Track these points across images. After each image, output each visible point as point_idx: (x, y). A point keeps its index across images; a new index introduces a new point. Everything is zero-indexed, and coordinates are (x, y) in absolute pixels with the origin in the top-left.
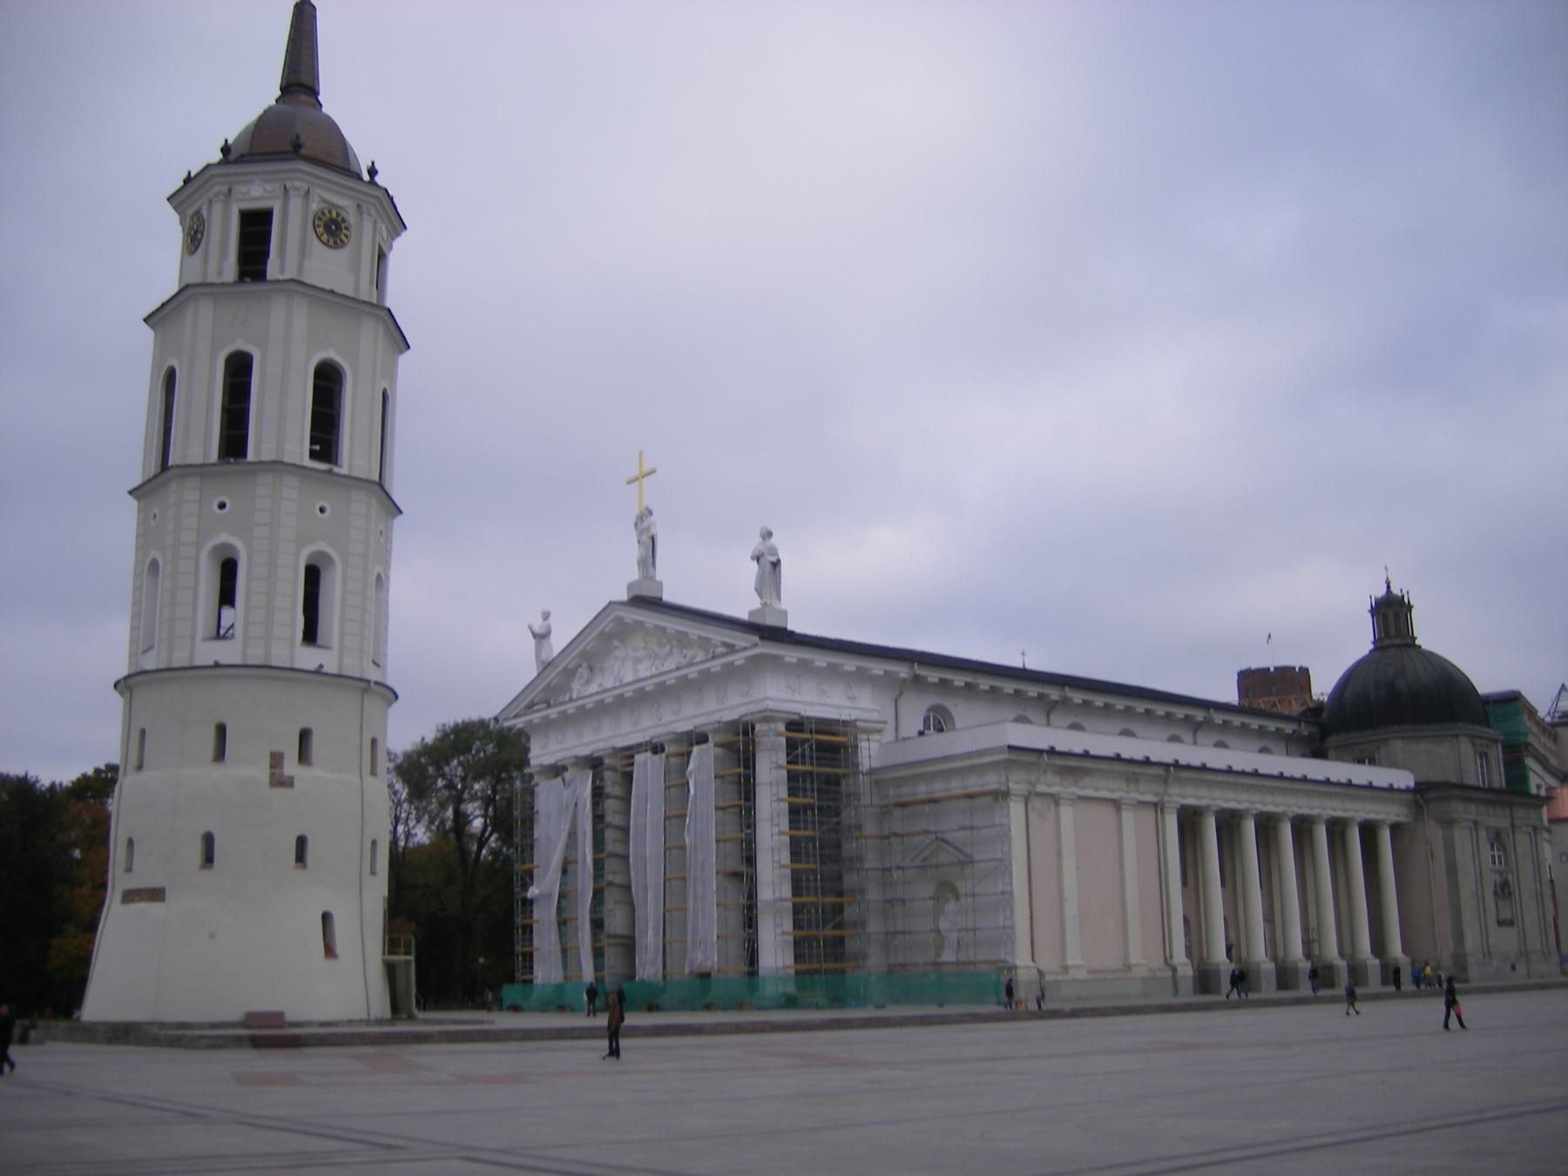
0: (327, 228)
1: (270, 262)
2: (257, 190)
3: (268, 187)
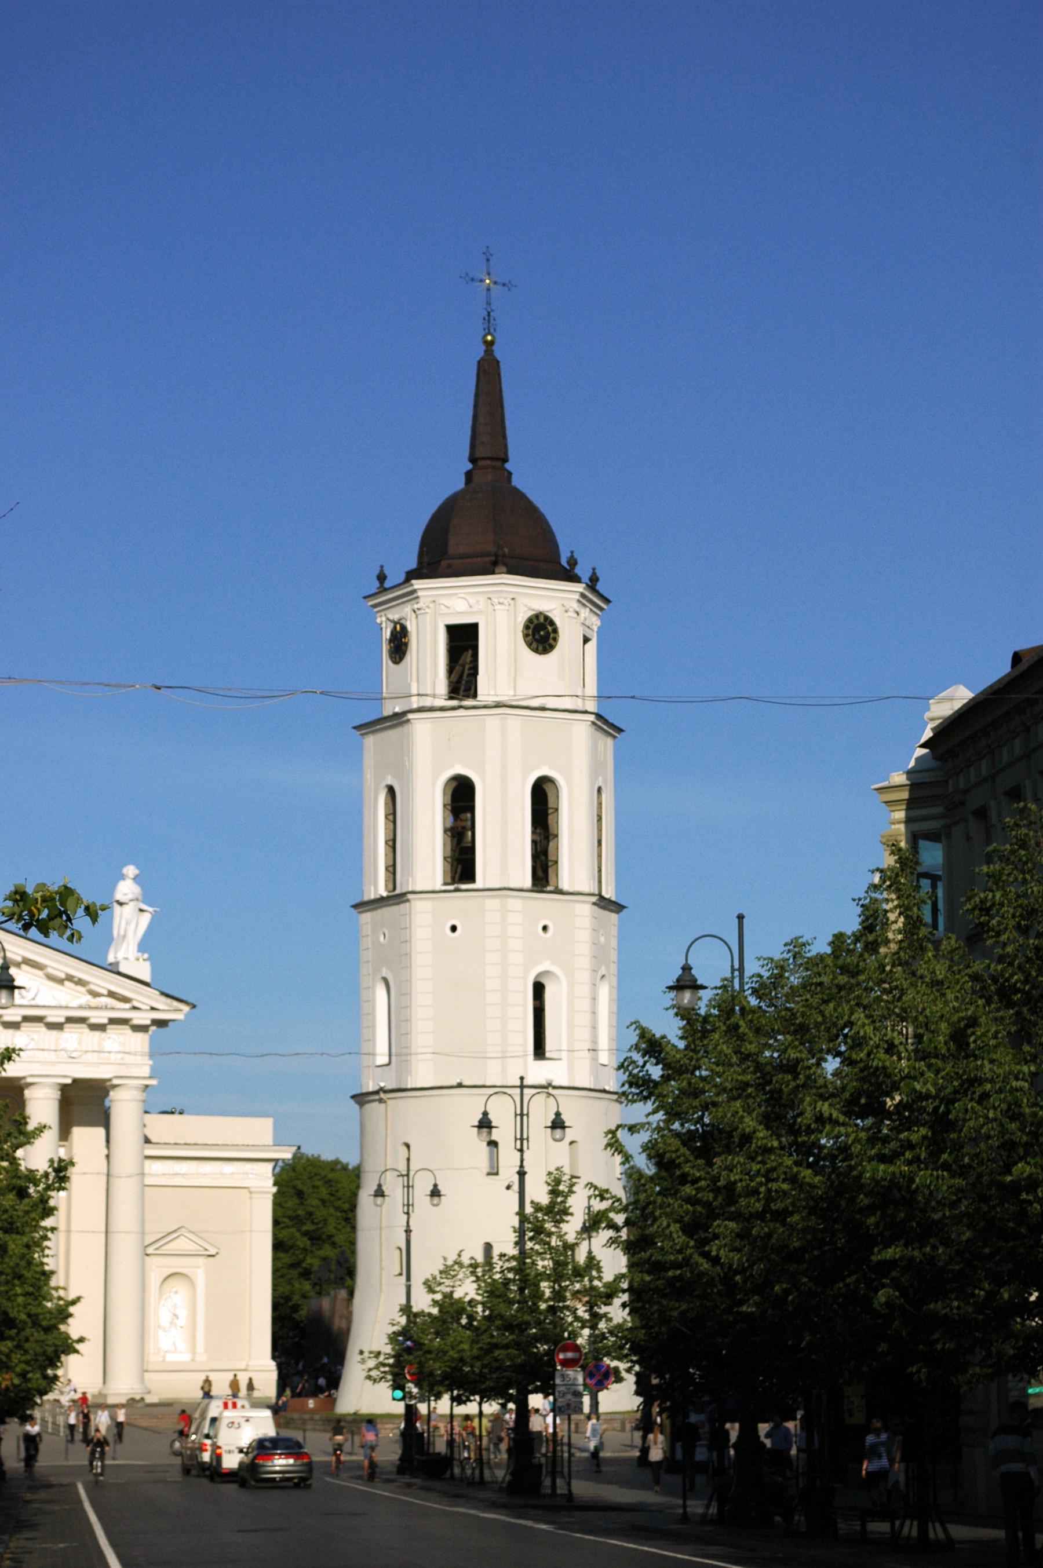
1: (479, 678)
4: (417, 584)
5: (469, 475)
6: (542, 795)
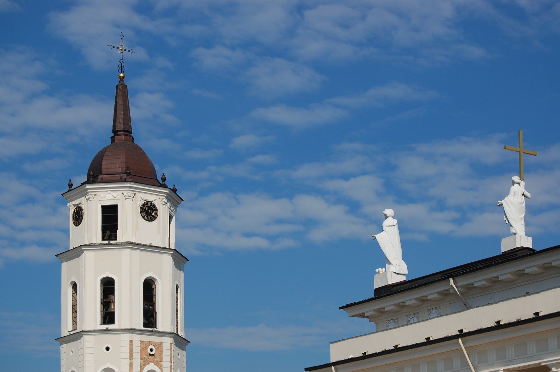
0: (147, 212)
4: (88, 186)
5: (113, 139)
6: (149, 287)
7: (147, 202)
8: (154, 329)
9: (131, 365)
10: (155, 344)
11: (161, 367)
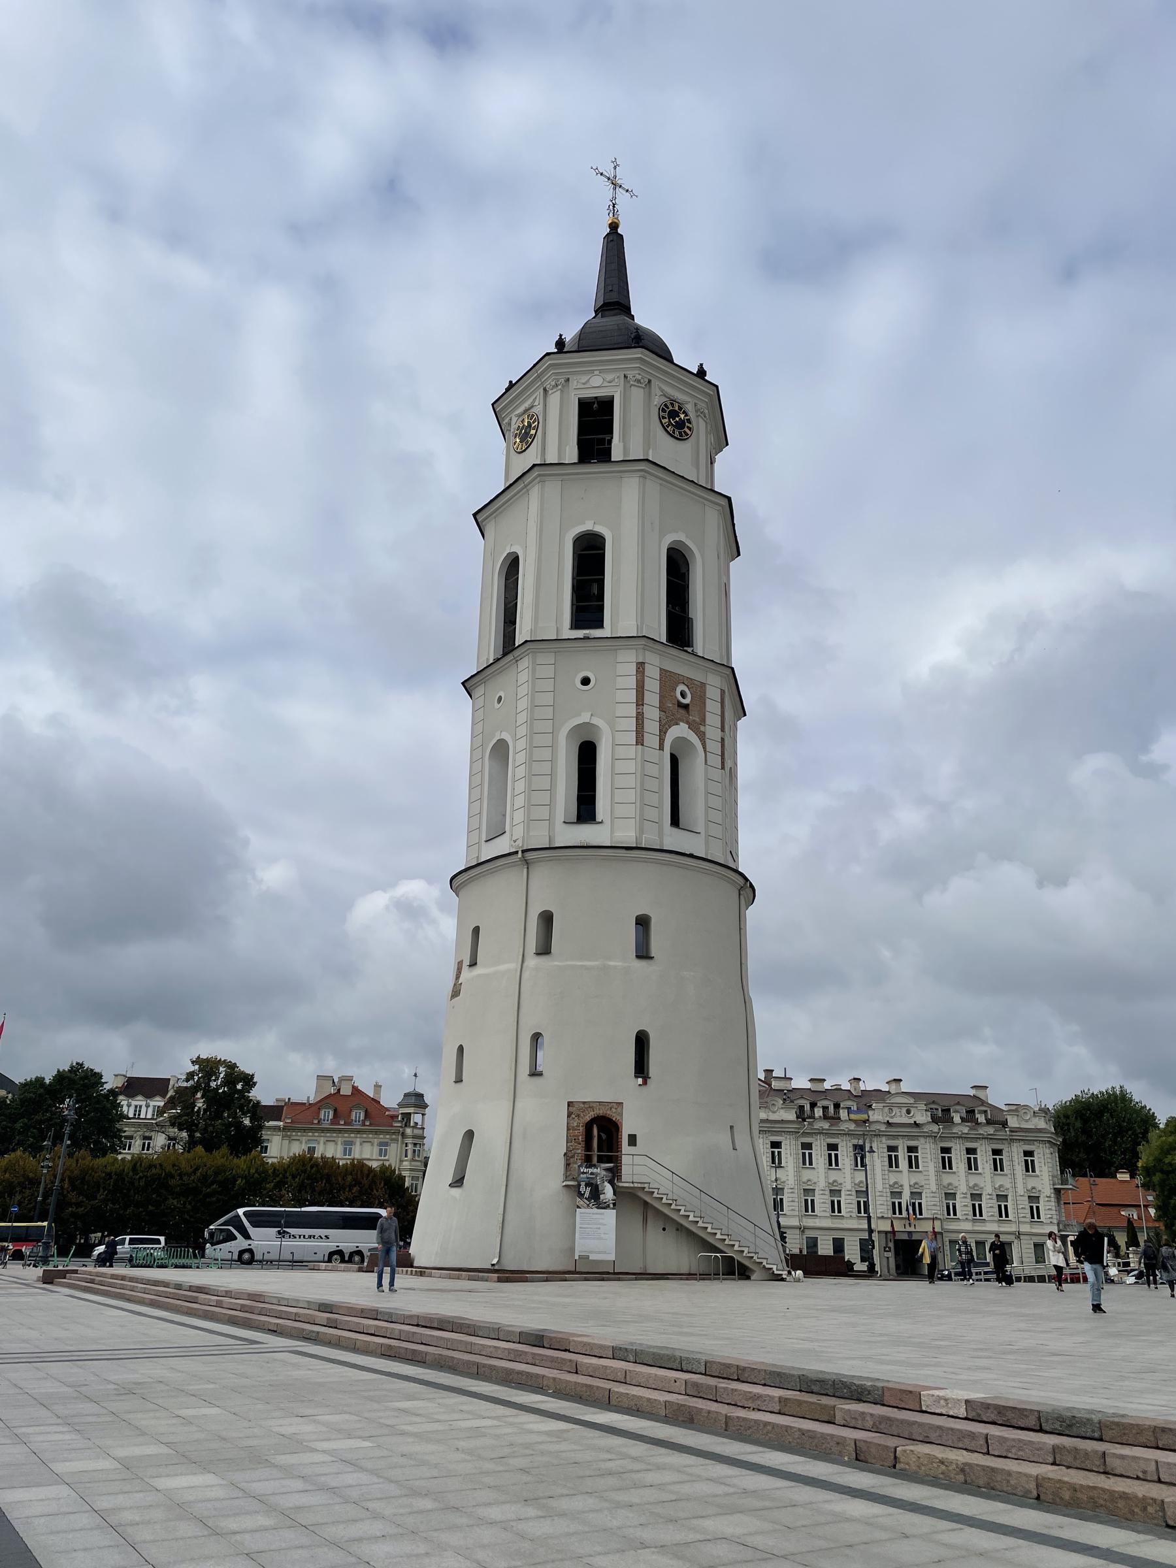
2: (596, 381)
3: (609, 377)
7: (673, 401)
8: (690, 650)
9: (640, 718)
10: (689, 682)
11: (702, 737)
